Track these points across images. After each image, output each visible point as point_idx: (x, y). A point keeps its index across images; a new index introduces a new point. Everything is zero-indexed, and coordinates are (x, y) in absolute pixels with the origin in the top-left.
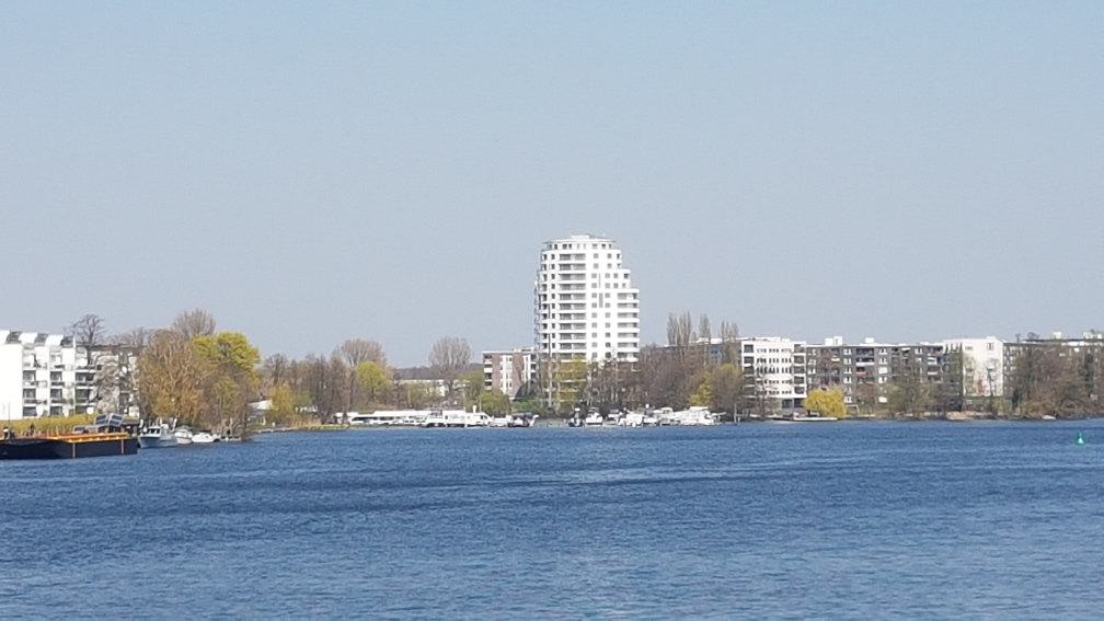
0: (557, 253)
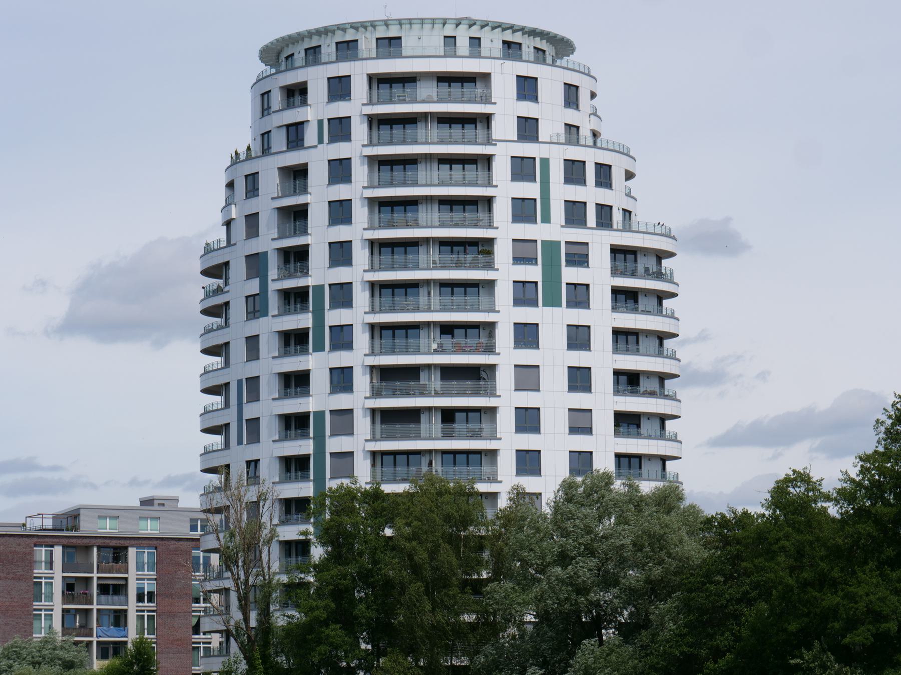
0: (358, 72)
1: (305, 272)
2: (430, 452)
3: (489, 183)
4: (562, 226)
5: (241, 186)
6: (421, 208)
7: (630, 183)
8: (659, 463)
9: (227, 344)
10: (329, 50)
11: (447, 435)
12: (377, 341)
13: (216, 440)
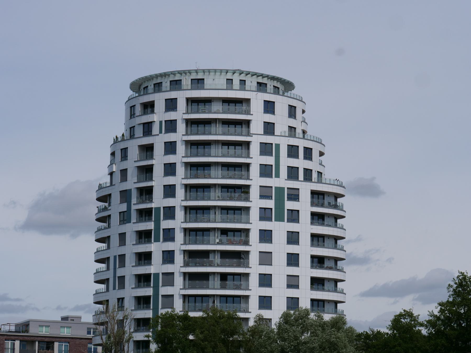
0: (181, 97)
1: (151, 200)
2: (214, 296)
3: (248, 156)
4: (286, 180)
5: (118, 155)
6: (212, 168)
7: (322, 158)
8: (333, 305)
9: (109, 237)
10: (166, 85)
11: (223, 287)
12: (187, 238)
13: (102, 287)
